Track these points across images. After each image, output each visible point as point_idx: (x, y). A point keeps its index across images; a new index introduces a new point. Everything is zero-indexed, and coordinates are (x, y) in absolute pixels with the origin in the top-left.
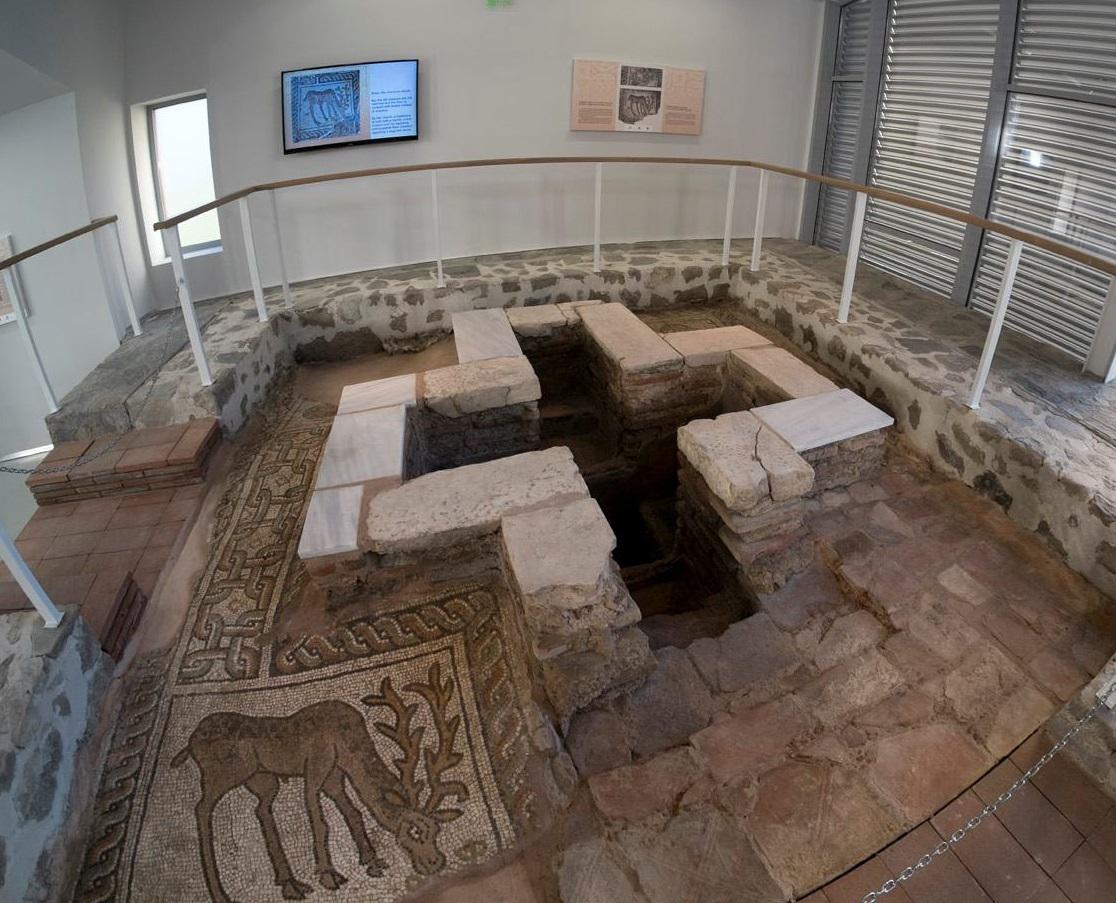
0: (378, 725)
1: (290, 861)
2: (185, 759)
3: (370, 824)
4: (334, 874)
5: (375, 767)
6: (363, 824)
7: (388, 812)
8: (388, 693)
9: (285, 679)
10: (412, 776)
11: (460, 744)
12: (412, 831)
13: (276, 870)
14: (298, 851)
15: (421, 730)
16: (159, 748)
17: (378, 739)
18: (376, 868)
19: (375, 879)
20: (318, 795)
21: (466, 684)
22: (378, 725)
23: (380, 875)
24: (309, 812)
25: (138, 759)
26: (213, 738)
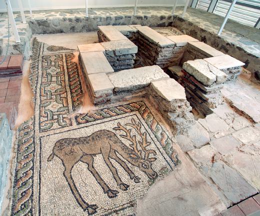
0: (120, 135)
1: (107, 183)
2: (53, 157)
3: (129, 165)
4: (124, 184)
5: (124, 147)
6: (127, 165)
7: (134, 160)
8: (121, 127)
9: (83, 125)
10: (137, 149)
11: (149, 139)
12: (144, 165)
13: (103, 188)
14: (107, 177)
15: (135, 136)
16: (40, 157)
18: (137, 180)
19: (138, 184)
20: (108, 159)
21: (144, 124)
22: (120, 135)
23: (139, 182)
24: (107, 165)
25: (31, 162)
26: (62, 148)
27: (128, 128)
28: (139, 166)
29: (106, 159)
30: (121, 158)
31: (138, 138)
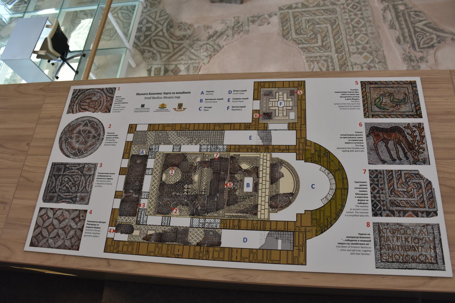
3: (406, 151)
15: (416, 136)
17: (407, 135)
27: (414, 129)
28: (411, 153)
29: (395, 144)
30: (403, 145)
31: (418, 138)
